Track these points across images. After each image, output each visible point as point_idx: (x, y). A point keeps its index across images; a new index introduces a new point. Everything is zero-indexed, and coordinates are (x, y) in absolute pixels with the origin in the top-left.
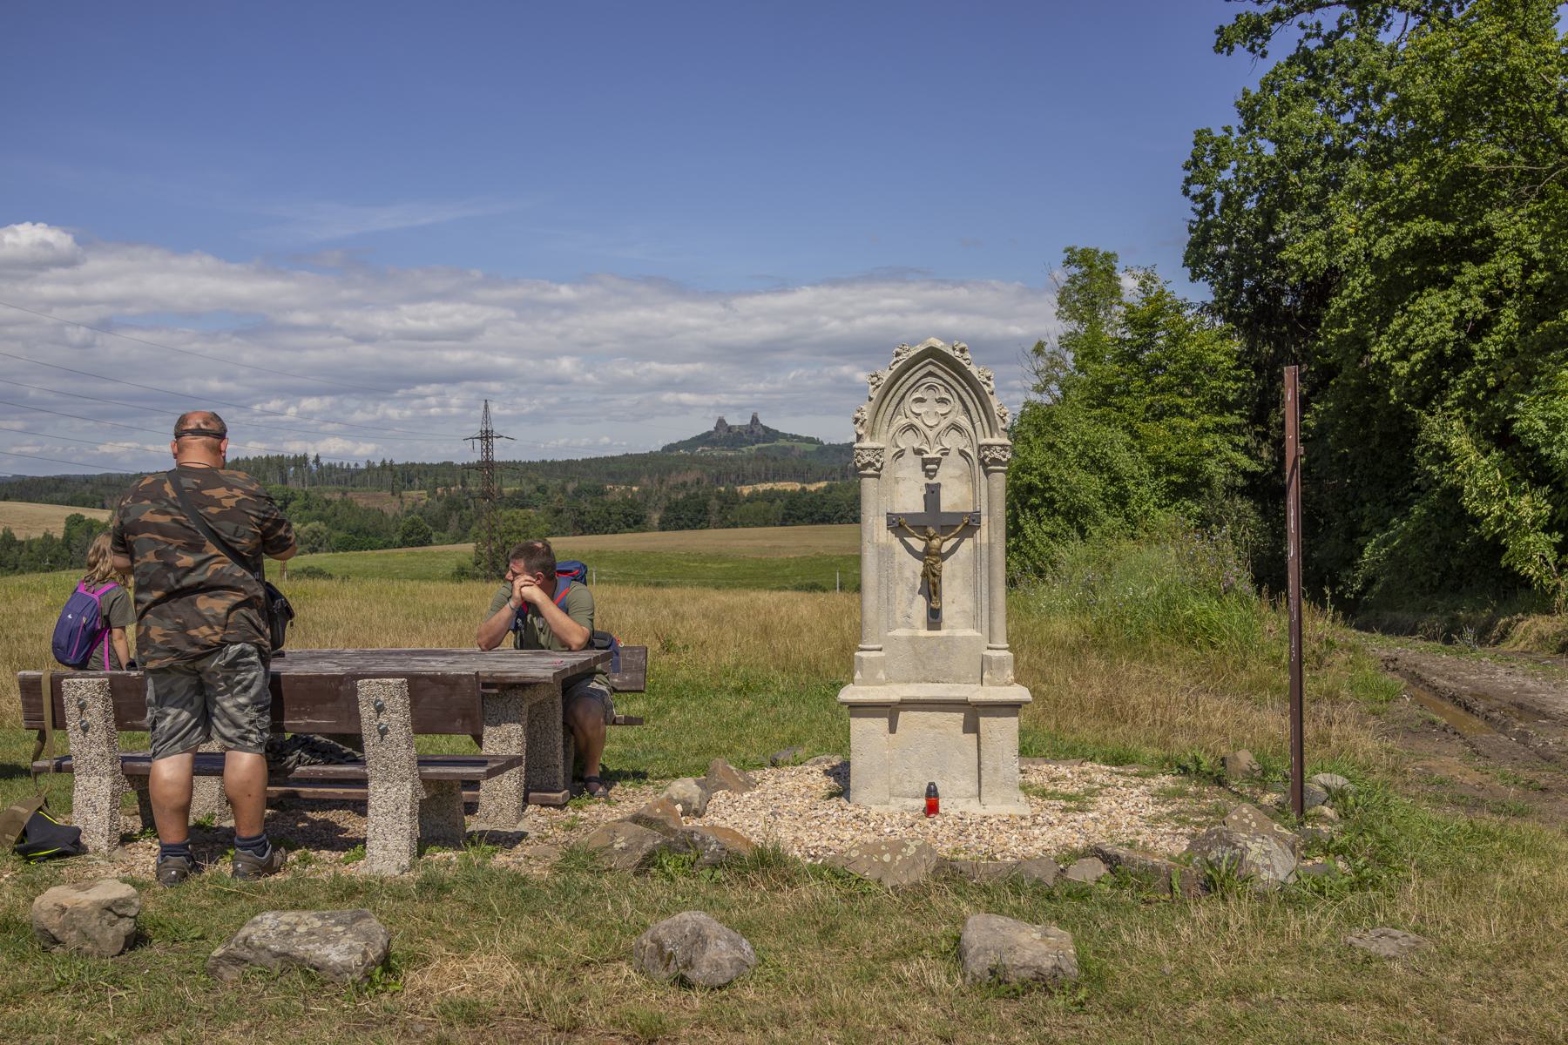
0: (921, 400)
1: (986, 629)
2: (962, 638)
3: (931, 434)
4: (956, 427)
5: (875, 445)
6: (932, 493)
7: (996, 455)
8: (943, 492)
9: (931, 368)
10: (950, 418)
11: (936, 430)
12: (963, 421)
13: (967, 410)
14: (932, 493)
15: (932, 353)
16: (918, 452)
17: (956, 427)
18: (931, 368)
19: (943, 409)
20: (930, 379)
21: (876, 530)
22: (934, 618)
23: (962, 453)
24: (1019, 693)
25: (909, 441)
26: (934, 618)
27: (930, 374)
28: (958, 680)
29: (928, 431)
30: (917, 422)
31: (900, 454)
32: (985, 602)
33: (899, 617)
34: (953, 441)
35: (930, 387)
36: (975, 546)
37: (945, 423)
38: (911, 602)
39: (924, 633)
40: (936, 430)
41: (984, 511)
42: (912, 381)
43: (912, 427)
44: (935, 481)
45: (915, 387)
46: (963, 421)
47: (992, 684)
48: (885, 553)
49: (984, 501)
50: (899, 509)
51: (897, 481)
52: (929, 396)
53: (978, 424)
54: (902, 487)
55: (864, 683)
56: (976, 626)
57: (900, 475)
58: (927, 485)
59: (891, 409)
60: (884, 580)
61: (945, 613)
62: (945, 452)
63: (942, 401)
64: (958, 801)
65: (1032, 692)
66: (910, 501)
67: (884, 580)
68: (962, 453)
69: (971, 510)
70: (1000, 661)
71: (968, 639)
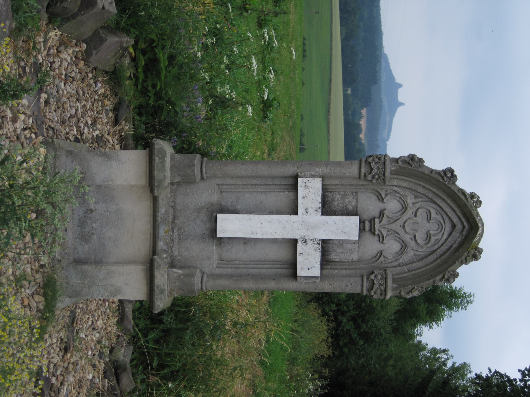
0: (429, 218)
3: (396, 226)
9: (459, 227)
11: (401, 231)
19: (420, 237)
27: (454, 226)
29: (400, 222)
30: (409, 213)
35: (441, 226)
37: (407, 238)
40: (401, 231)
42: (447, 209)
63: (428, 237)
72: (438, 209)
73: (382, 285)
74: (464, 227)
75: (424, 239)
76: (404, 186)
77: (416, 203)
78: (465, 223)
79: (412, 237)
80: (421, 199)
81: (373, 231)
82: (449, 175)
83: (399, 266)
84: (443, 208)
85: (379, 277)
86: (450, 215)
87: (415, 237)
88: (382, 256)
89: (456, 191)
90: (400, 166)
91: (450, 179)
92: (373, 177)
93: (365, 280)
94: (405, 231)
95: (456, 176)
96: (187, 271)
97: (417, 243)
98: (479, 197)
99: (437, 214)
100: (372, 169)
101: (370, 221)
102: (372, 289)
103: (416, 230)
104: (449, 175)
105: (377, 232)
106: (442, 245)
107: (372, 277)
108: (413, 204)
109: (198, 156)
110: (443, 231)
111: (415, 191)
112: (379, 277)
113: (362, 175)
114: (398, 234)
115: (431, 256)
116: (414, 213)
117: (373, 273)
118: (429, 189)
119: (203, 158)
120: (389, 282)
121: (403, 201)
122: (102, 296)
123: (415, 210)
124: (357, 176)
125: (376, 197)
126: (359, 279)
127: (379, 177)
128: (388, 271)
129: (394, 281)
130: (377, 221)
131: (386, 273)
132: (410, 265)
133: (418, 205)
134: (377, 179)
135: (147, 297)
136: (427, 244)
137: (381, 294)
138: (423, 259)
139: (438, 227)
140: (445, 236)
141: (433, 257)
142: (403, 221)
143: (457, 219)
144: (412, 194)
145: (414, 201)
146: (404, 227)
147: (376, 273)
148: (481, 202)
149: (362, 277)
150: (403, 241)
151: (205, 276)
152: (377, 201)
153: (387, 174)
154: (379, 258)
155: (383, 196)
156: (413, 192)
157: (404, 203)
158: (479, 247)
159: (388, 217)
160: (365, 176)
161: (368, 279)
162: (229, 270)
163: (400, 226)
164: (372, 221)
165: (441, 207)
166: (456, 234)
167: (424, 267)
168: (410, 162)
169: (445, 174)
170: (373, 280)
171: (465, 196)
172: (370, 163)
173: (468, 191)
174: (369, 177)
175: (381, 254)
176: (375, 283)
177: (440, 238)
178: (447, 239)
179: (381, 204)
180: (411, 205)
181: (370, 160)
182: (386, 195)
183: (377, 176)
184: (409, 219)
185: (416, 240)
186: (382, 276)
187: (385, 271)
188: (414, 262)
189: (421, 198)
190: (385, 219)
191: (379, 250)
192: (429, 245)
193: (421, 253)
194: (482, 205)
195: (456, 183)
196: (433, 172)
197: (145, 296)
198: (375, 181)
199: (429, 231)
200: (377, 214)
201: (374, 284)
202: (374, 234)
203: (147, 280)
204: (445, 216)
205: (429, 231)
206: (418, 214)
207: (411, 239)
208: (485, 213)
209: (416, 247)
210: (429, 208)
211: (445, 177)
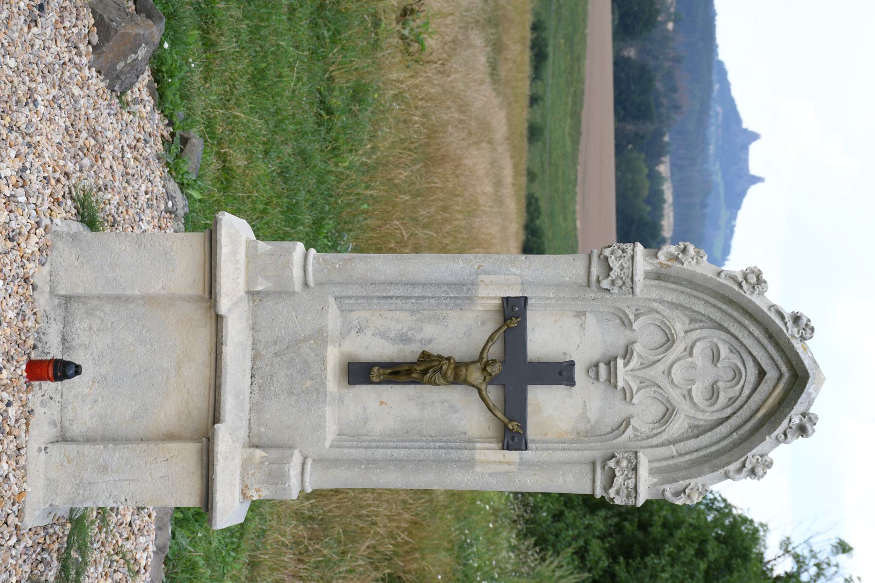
0: (715, 358)
1: (336, 453)
2: (322, 417)
3: (656, 373)
4: (668, 414)
5: (639, 277)
6: (560, 373)
7: (619, 480)
10: (683, 406)
11: (663, 382)
13: (698, 431)
14: (560, 373)
15: (798, 378)
16: (627, 353)
17: (668, 414)
19: (699, 392)
20: (751, 373)
22: (359, 373)
23: (626, 423)
24: (229, 511)
25: (645, 334)
26: (359, 373)
27: (762, 374)
28: (255, 408)
29: (661, 367)
30: (678, 348)
31: (626, 323)
32: (379, 453)
33: (357, 316)
34: (644, 411)
35: (737, 375)
36: (470, 442)
37: (675, 395)
38: (383, 335)
39: (333, 357)
40: (663, 382)
42: (749, 342)
43: (669, 341)
44: (579, 374)
45: (738, 347)
46: (678, 426)
47: (246, 464)
48: (461, 293)
49: (545, 456)
51: (580, 314)
52: (723, 372)
53: (673, 450)
54: (570, 323)
55: (252, 256)
57: (591, 320)
58: (572, 364)
59: (700, 307)
60: (418, 292)
61: (365, 391)
62: (626, 395)
63: (713, 393)
64: (55, 407)
66: (544, 339)
67: (418, 292)
68: (626, 423)
69: (531, 434)
70: (278, 477)
71: (320, 427)
72: (736, 345)
73: (629, 479)
74: (781, 375)
75: (708, 397)
76: (669, 299)
77: (692, 330)
78: (784, 368)
79: (686, 393)
80: (701, 324)
81: (612, 381)
82: (753, 279)
83: (662, 445)
84: (742, 339)
85: (624, 464)
86: (755, 353)
87: (690, 391)
88: (631, 427)
89: (765, 309)
90: (661, 263)
91: (754, 287)
92: (613, 283)
93: (599, 470)
94: (672, 382)
95: (765, 282)
96: (275, 454)
97: (694, 404)
98: (809, 321)
99: (731, 351)
100: (611, 269)
101: (608, 364)
102: (611, 486)
103: (692, 381)
104: (753, 279)
105: (620, 384)
106: (741, 407)
107: (612, 464)
108: (686, 332)
109: (300, 246)
110: (742, 382)
111: (690, 309)
112: (624, 464)
113: (594, 278)
114: (659, 387)
115: (721, 427)
116: (688, 350)
117: (614, 456)
118: (714, 306)
119: (307, 249)
120: (643, 471)
121: (669, 327)
122: (115, 502)
123: (689, 342)
124: (585, 280)
125: (618, 321)
126: (588, 469)
127: (624, 283)
128: (640, 454)
129: (652, 472)
130: (620, 362)
131: (636, 457)
132: (682, 444)
133: (694, 335)
134: (620, 287)
135: (201, 502)
136: (712, 405)
137: (628, 496)
138: (705, 432)
139: (733, 374)
140: (746, 392)
141: (723, 429)
142: (669, 363)
143: (769, 361)
144: (686, 315)
145: (687, 327)
146: (669, 373)
147: (619, 457)
148: (812, 329)
149: (593, 464)
150: (668, 401)
151: (309, 462)
152: (622, 328)
153: (636, 279)
154: (624, 432)
155: (632, 317)
156: (687, 312)
157: (670, 330)
158: (811, 411)
159: (640, 356)
160: (598, 281)
161: (603, 467)
162: (353, 451)
163: (663, 373)
164: (612, 363)
165: (737, 339)
166: (764, 388)
167: (707, 447)
168: (680, 256)
169: (746, 279)
170: (614, 470)
171: (783, 318)
172: (606, 258)
173: (788, 310)
174: (605, 284)
175: (628, 424)
176: (617, 474)
177: (738, 394)
178: (749, 397)
179: (628, 332)
180: (683, 334)
181: (607, 252)
182: (637, 316)
183: (620, 282)
184: (679, 359)
185: (691, 399)
186: (629, 461)
187: (636, 453)
188: (688, 438)
189: (701, 321)
190: (634, 362)
191: (624, 416)
192: (716, 407)
193: (702, 423)
194: (815, 334)
195: (766, 294)
196: (723, 275)
197: (198, 500)
198: (616, 290)
199: (716, 382)
200: (621, 351)
201: (615, 476)
202: (616, 387)
203: (202, 467)
204: (745, 355)
205: (716, 382)
206: (695, 350)
207: (684, 396)
208: (816, 351)
209: (692, 412)
210: (715, 340)
211: (744, 284)
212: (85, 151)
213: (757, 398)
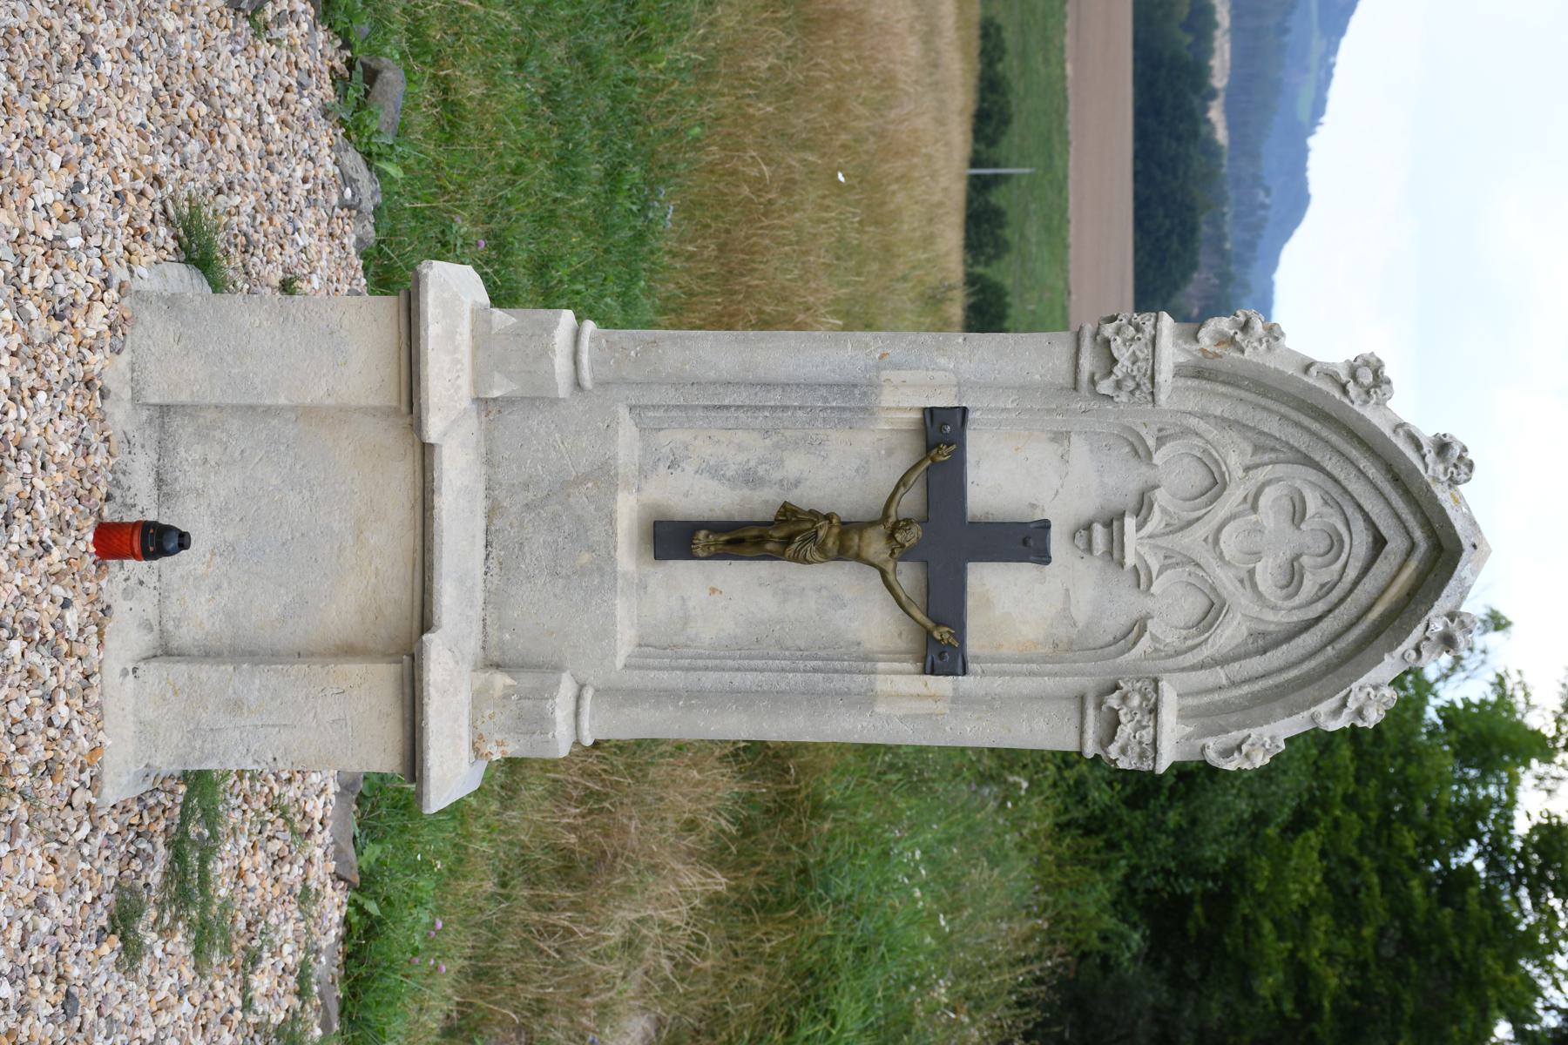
0: (1298, 514)
1: (635, 679)
2: (610, 616)
4: (1214, 611)
5: (1165, 375)
6: (1025, 541)
7: (1125, 730)
8: (1023, 572)
9: (1396, 544)
10: (1240, 599)
11: (1206, 556)
12: (1229, 633)
13: (1265, 642)
14: (1025, 541)
15: (1442, 552)
16: (1143, 506)
17: (1214, 611)
18: (1396, 544)
19: (1267, 574)
20: (1361, 542)
21: (940, 366)
22: (673, 539)
23: (1139, 627)
24: (451, 776)
25: (1174, 472)
26: (673, 539)
27: (1379, 542)
28: (494, 599)
29: (1201, 531)
30: (1233, 498)
31: (1141, 453)
32: (709, 680)
33: (670, 439)
34: (1171, 606)
35: (1335, 544)
36: (866, 660)
37: (1226, 580)
38: (715, 472)
39: (628, 511)
40: (1206, 556)
41: (965, 682)
42: (1356, 487)
43: (1216, 485)
44: (1058, 543)
45: (1338, 496)
46: (1229, 633)
47: (479, 699)
48: (850, 400)
49: (997, 685)
50: (977, 444)
51: (1060, 437)
52: (1310, 537)
53: (1220, 675)
54: (1041, 452)
55: (482, 337)
56: (650, 649)
57: (1079, 446)
58: (1045, 525)
59: (1272, 426)
60: (775, 398)
61: (681, 569)
62: (1141, 579)
63: (1293, 576)
64: (148, 597)
65: (457, 810)
66: (996, 480)
67: (775, 398)
68: (1139, 627)
69: (973, 645)
70: (536, 722)
71: (605, 633)
72: (1335, 492)
73: (1144, 727)
74: (1413, 546)
75: (1284, 582)
76: (1218, 413)
77: (1257, 466)
78: (1418, 534)
79: (1244, 575)
80: (1273, 456)
81: (1116, 555)
82: (1367, 377)
83: (1202, 666)
84: (1345, 483)
85: (1135, 701)
86: (1368, 507)
87: (1252, 572)
88: (1147, 635)
89: (1388, 432)
90: (1203, 351)
91: (1368, 393)
92: (1118, 385)
93: (1091, 712)
94: (1221, 556)
95: (1389, 382)
96: (528, 680)
97: (1260, 595)
98: (1465, 449)
99: (1326, 503)
100: (1115, 361)
101: (1108, 524)
102: (1111, 740)
103: (1257, 555)
104: (1367, 377)
105: (1130, 560)
106: (1342, 600)
107: (1113, 701)
108: (1247, 469)
109: (568, 316)
111: (1254, 428)
112: (1135, 701)
113: (1084, 376)
114: (1198, 565)
115: (1305, 636)
116: (1250, 500)
117: (1116, 687)
118: (1297, 424)
119: (579, 318)
120: (1168, 715)
121: (1216, 461)
122: (256, 762)
123: (1251, 486)
124: (1069, 380)
125: (1127, 449)
126: (1071, 709)
127: (1138, 386)
128: (1163, 685)
129: (1184, 715)
130: (1130, 523)
131: (1156, 690)
132: (1236, 665)
133: (1261, 475)
134: (1132, 393)
135: (402, 764)
136: (1290, 597)
137: (1142, 756)
138: (1277, 644)
139: (1328, 542)
140: (1352, 573)
141: (1309, 640)
142: (1215, 523)
143: (1392, 522)
144: (1246, 439)
145: (1248, 460)
146: (1216, 541)
147: (1125, 688)
148: (1471, 466)
149: (1082, 699)
150: (1214, 589)
151: (588, 694)
152: (1133, 462)
153: (1160, 378)
154: (1135, 644)
155: (1151, 443)
156: (1250, 434)
157: (1219, 466)
158: (1462, 609)
159: (1164, 511)
160: (1093, 382)
161: (1099, 706)
162: (665, 675)
163: (1205, 540)
164: (1115, 524)
165: (1336, 481)
166: (1383, 568)
167: (1280, 670)
168: (1239, 337)
169: (1354, 376)
170: (1116, 712)
171: (1418, 446)
172: (1107, 342)
173: (1428, 431)
174: (1105, 387)
175: (1143, 630)
176: (1123, 719)
177: (1336, 577)
178: (1356, 583)
179: (1144, 469)
180: (1241, 473)
181: (1108, 330)
182: (1161, 441)
183: (1131, 384)
184: (1233, 517)
185: (1254, 585)
186: (1144, 697)
187: (1156, 681)
188: (1247, 655)
189: (1273, 449)
190: (1155, 522)
191: (1136, 616)
192: (1297, 600)
193: (1271, 628)
194: (1474, 475)
195: (1388, 404)
196: (1313, 370)
197: (398, 761)
198: (1123, 397)
199: (1297, 557)
200: (1132, 502)
201: (1119, 723)
202: (1122, 565)
203: (403, 706)
204: (1350, 510)
205: (1297, 557)
206: (1262, 502)
207: (1241, 581)
208: (1479, 504)
209: (1255, 610)
210: (1298, 484)
211: (1351, 386)
212: (191, 128)
213: (1370, 585)
